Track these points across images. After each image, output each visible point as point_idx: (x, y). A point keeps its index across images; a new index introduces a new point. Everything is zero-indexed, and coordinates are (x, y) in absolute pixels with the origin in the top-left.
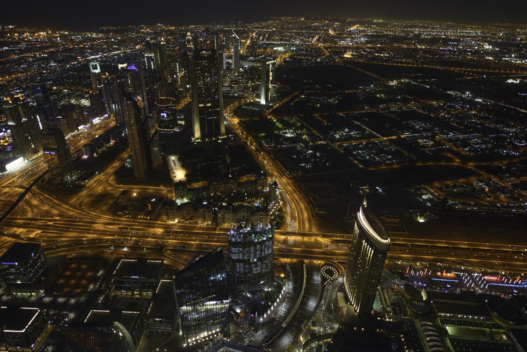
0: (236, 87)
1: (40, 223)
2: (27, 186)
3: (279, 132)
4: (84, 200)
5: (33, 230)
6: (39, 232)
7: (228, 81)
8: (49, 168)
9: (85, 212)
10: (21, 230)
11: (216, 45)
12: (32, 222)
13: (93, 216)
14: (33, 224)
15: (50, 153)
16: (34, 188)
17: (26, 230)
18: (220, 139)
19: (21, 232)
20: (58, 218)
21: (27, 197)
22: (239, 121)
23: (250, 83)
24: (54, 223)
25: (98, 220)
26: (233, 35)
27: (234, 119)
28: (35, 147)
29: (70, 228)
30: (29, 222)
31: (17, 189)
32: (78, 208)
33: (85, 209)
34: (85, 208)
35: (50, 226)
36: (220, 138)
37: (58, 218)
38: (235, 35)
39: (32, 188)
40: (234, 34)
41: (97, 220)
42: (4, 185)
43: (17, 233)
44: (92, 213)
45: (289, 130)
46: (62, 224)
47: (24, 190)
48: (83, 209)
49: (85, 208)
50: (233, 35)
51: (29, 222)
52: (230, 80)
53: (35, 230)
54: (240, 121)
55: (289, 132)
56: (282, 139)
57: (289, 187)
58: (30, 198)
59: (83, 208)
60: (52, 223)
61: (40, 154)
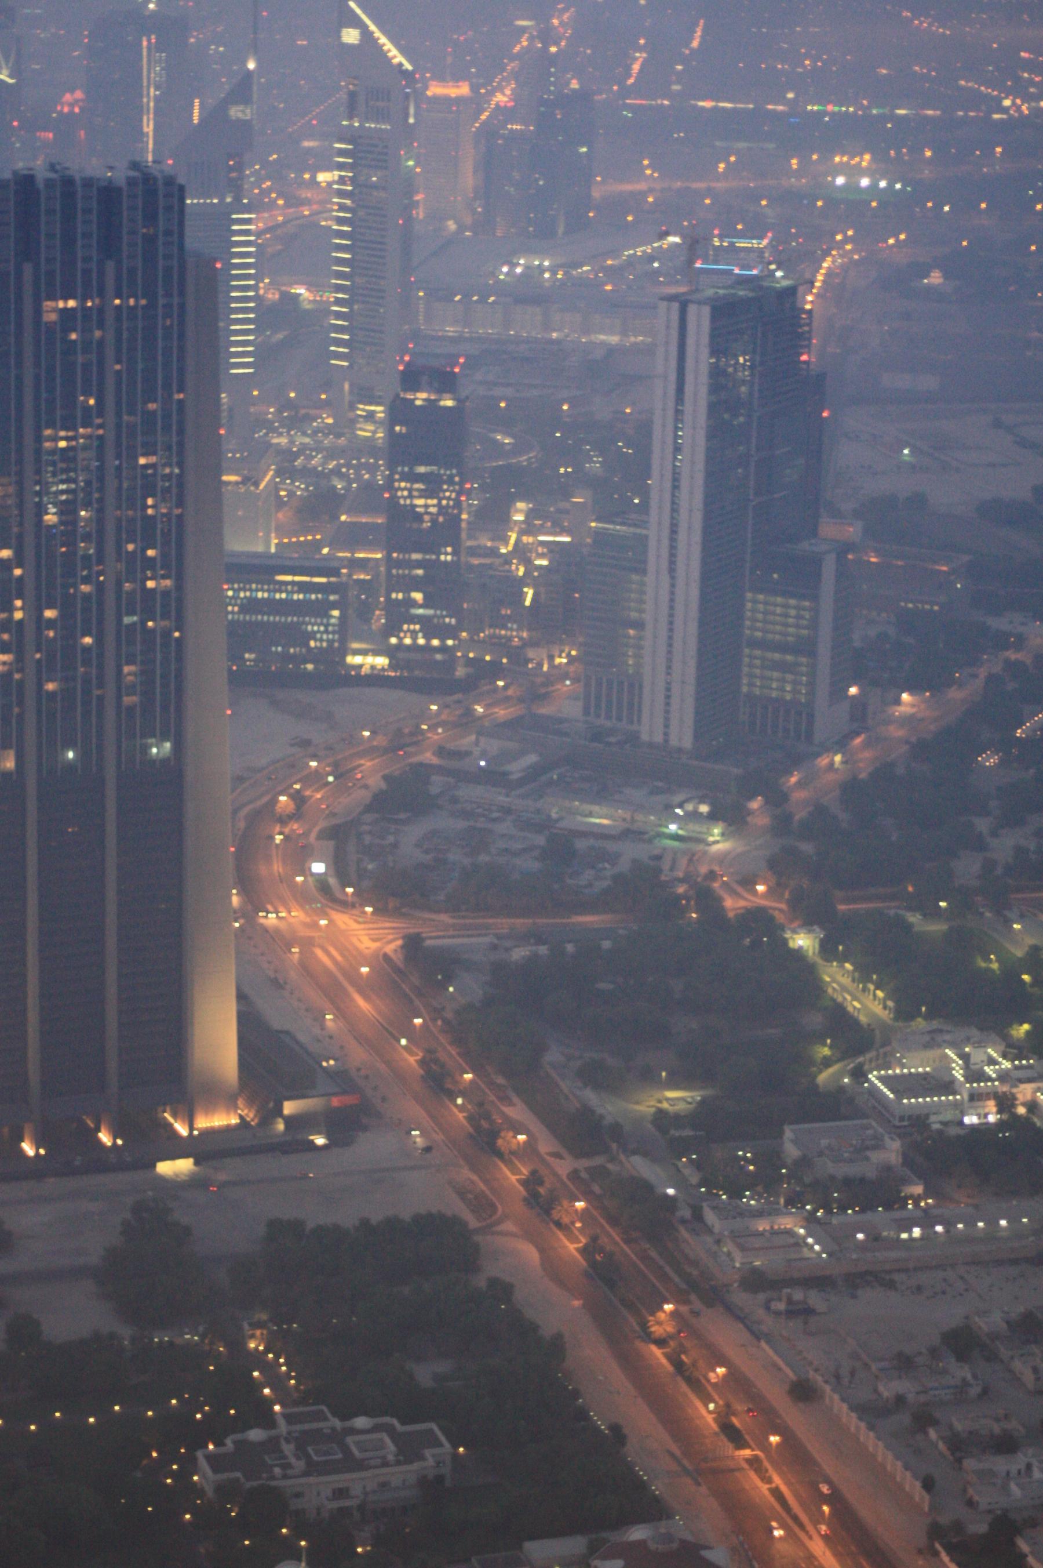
0: (363, 564)
3: (859, 1074)
7: (280, 503)
11: (149, 127)
18: (176, 1148)
22: (393, 947)
23: (528, 528)
26: (351, 36)
27: (343, 920)
36: (182, 1130)
38: (366, 34)
40: (358, 23)
45: (977, 1056)
50: (351, 36)
52: (300, 488)
54: (413, 945)
55: (975, 1075)
56: (892, 1152)
57: (828, 979)
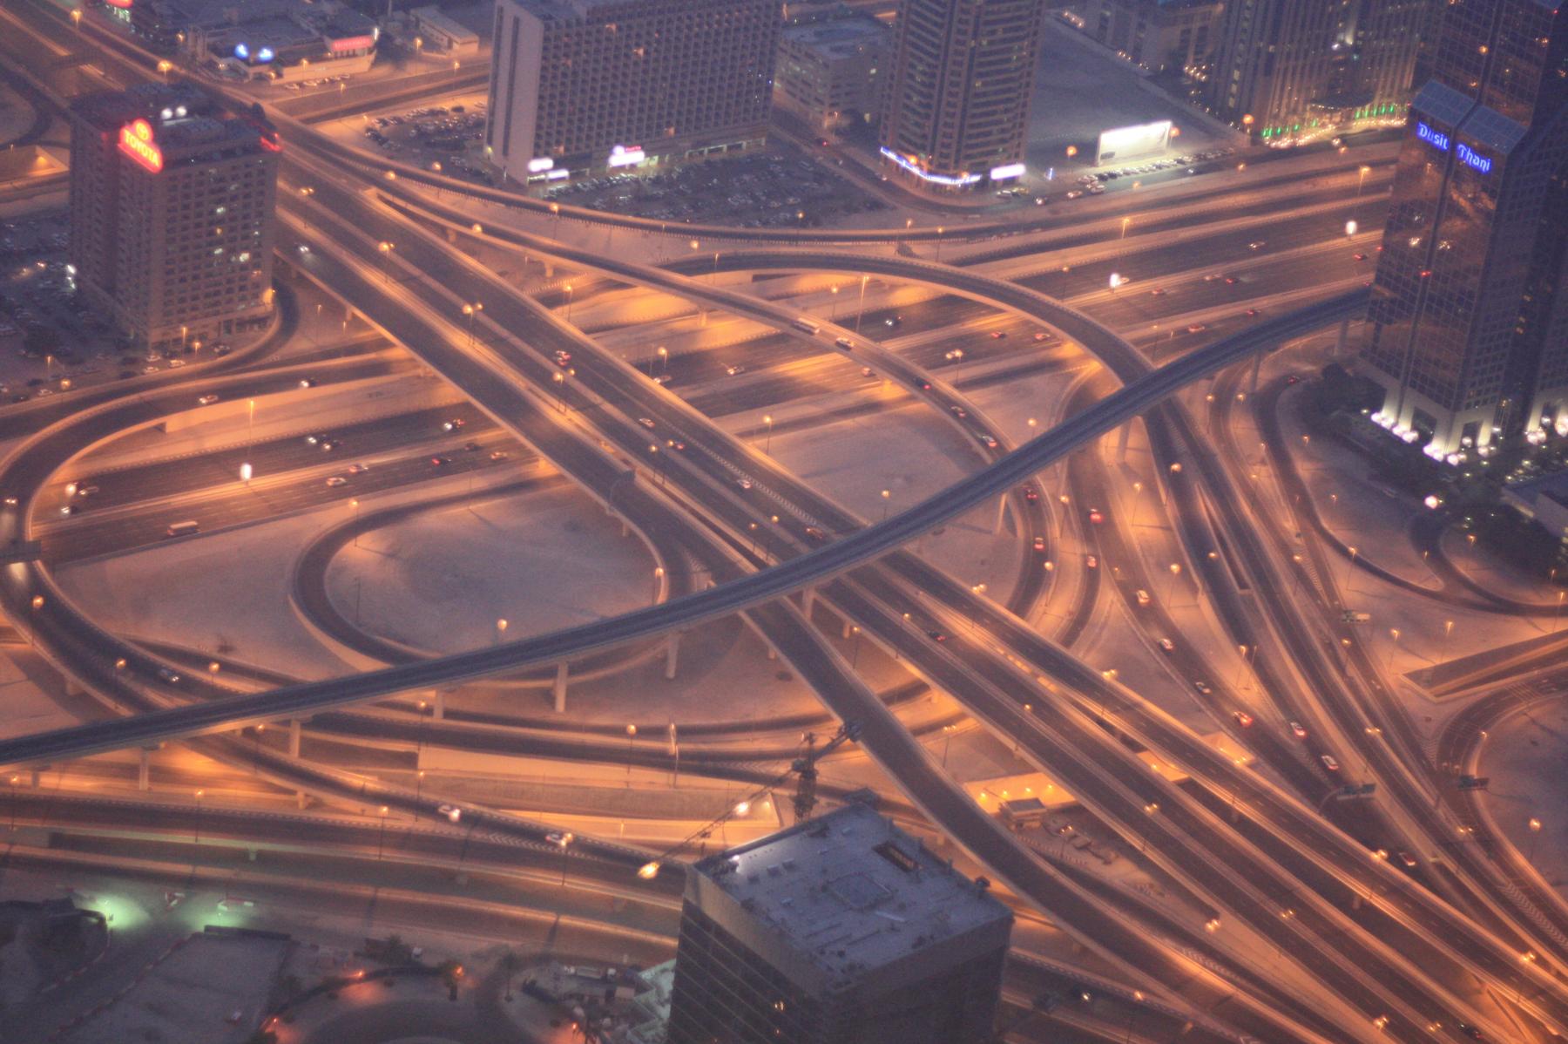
1: (1085, 715)
2: (1146, 359)
4: (1514, 701)
5: (1022, 753)
6: (1051, 792)
8: (1378, 280)
9: (1469, 815)
10: (943, 703)
12: (1047, 684)
13: (1512, 890)
14: (1043, 706)
15: (1453, 146)
16: (1196, 398)
17: (973, 723)
19: (933, 728)
20: (1238, 757)
21: (1109, 444)
24: (1188, 786)
25: (1540, 961)
28: (1355, 49)
29: (1286, 897)
30: (1021, 666)
31: (1070, 349)
32: (1431, 751)
33: (1478, 795)
34: (1482, 783)
35: (1150, 788)
37: (1238, 757)
39: (1183, 394)
41: (1524, 948)
42: (1003, 273)
43: (904, 716)
44: (1520, 860)
46: (1241, 824)
47: (1113, 385)
48: (1468, 783)
49: (1482, 783)
51: (1021, 666)
53: (1032, 761)
58: (1124, 467)
59: (1473, 771)
60: (1167, 770)
61: (1364, 121)
